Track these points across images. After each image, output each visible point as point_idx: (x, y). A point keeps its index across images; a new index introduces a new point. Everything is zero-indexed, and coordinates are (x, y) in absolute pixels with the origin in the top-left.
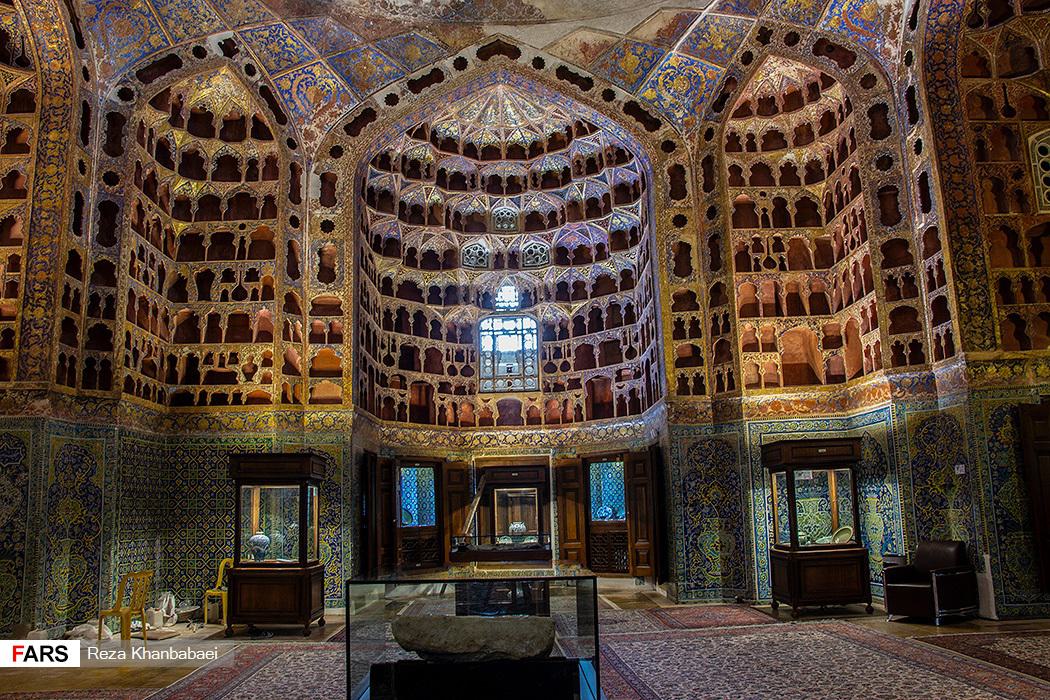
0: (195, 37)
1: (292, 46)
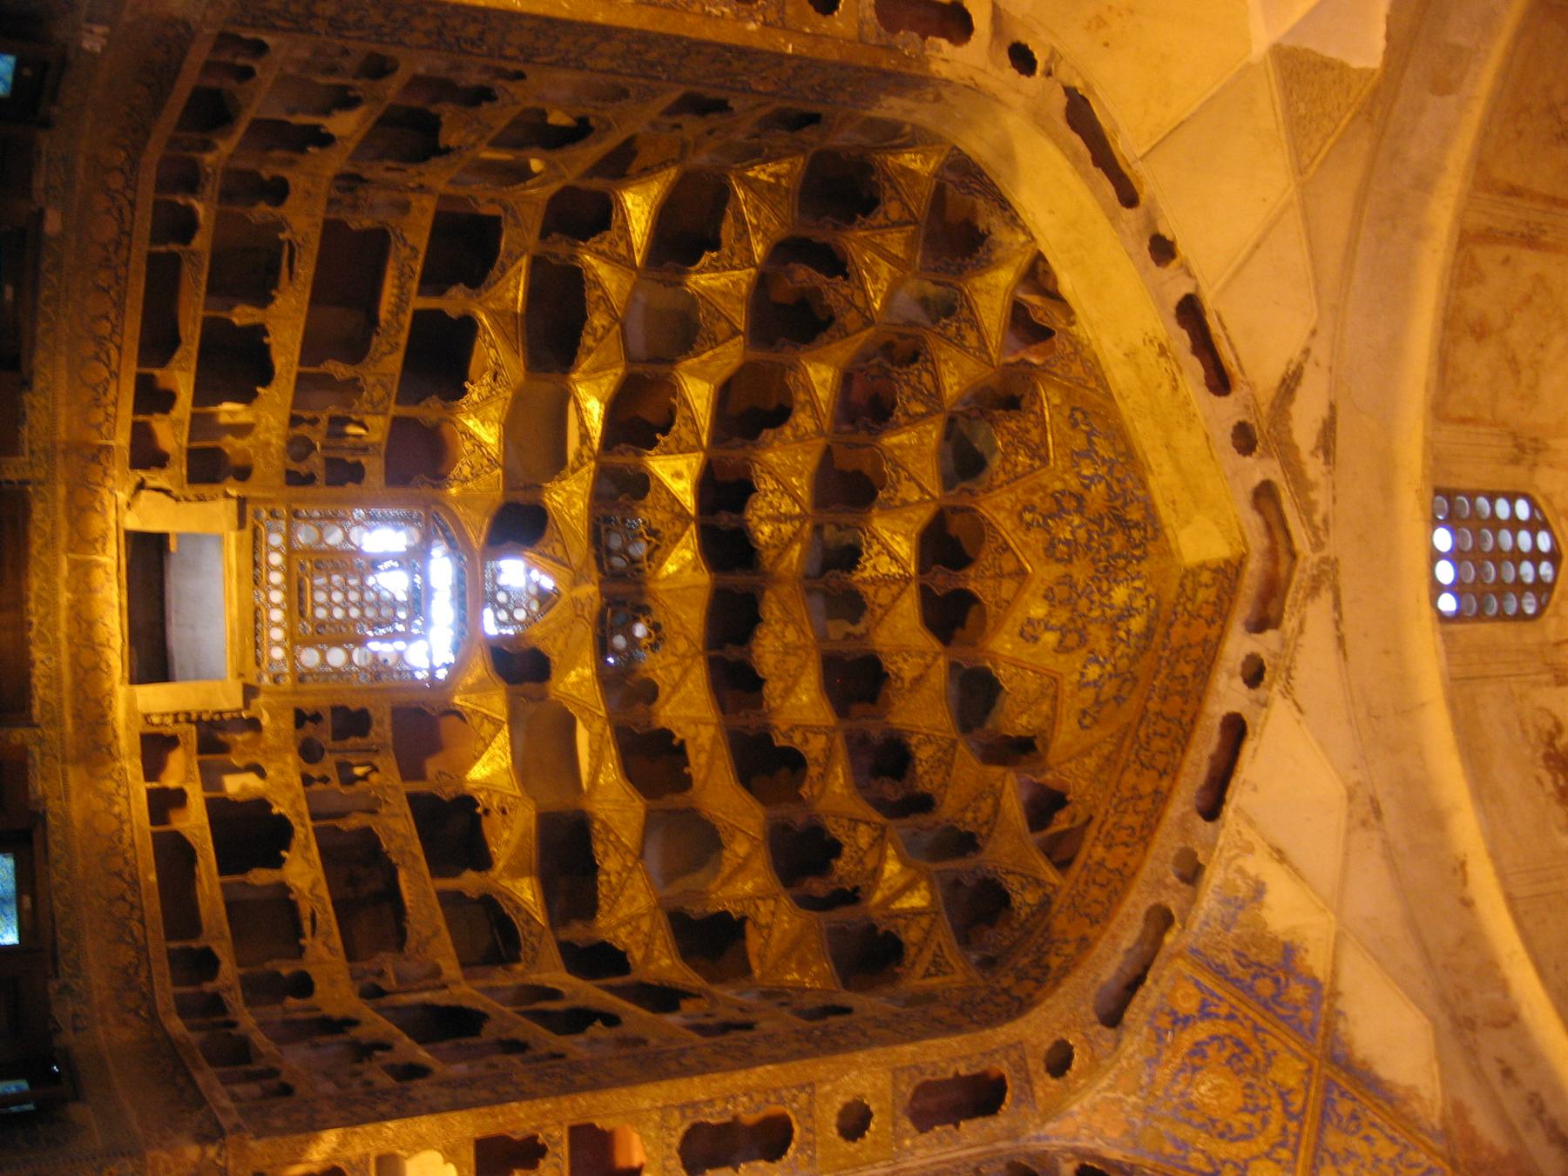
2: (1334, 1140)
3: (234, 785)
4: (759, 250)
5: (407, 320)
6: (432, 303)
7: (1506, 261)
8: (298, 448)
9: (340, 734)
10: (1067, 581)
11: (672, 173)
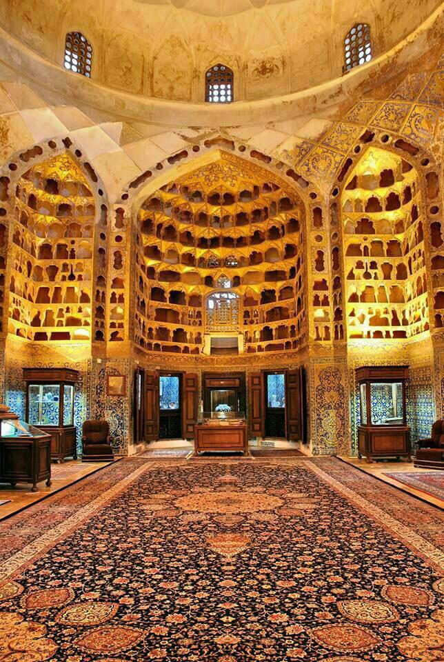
0: (353, 142)
1: (399, 109)
2: (333, 144)
3: (258, 336)
4: (158, 241)
5: (171, 304)
6: (168, 299)
7: (156, 82)
8: (194, 324)
9: (249, 317)
10: (223, 178)
11: (144, 258)
